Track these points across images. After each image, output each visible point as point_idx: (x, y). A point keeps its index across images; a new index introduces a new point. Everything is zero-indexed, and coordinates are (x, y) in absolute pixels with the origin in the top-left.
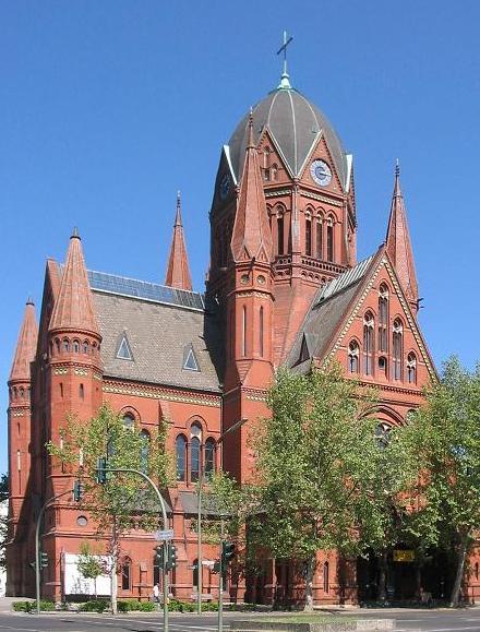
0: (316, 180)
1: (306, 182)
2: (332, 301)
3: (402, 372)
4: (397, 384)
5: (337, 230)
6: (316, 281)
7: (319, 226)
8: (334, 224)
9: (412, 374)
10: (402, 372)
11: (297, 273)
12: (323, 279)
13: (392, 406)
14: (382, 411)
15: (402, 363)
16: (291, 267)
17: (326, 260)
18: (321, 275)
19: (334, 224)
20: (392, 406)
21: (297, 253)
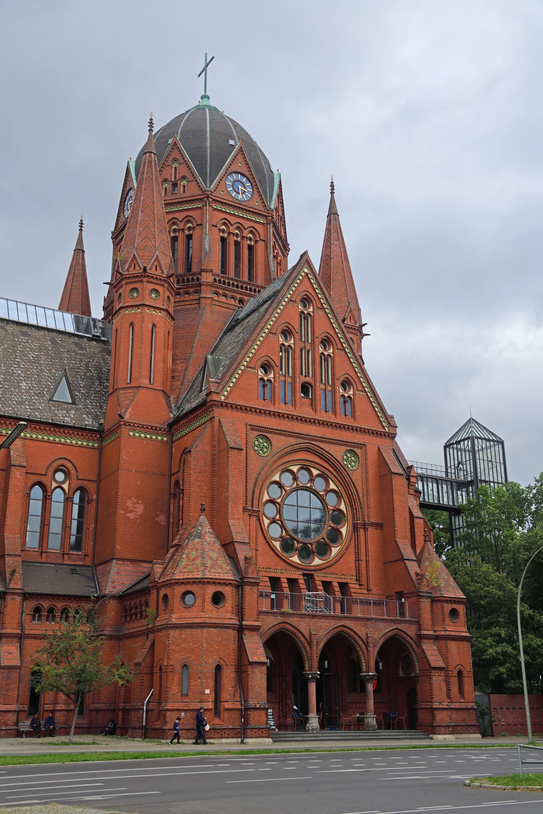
0: (234, 194)
1: (220, 194)
2: (246, 321)
3: (334, 403)
4: (329, 417)
5: (260, 248)
6: (232, 301)
7: (237, 243)
8: (256, 242)
9: (348, 406)
10: (334, 403)
11: (206, 293)
12: (241, 301)
13: (322, 445)
14: (307, 450)
15: (334, 392)
16: (200, 285)
17: (246, 279)
18: (238, 296)
19: (256, 242)
20: (322, 445)
21: (206, 271)
